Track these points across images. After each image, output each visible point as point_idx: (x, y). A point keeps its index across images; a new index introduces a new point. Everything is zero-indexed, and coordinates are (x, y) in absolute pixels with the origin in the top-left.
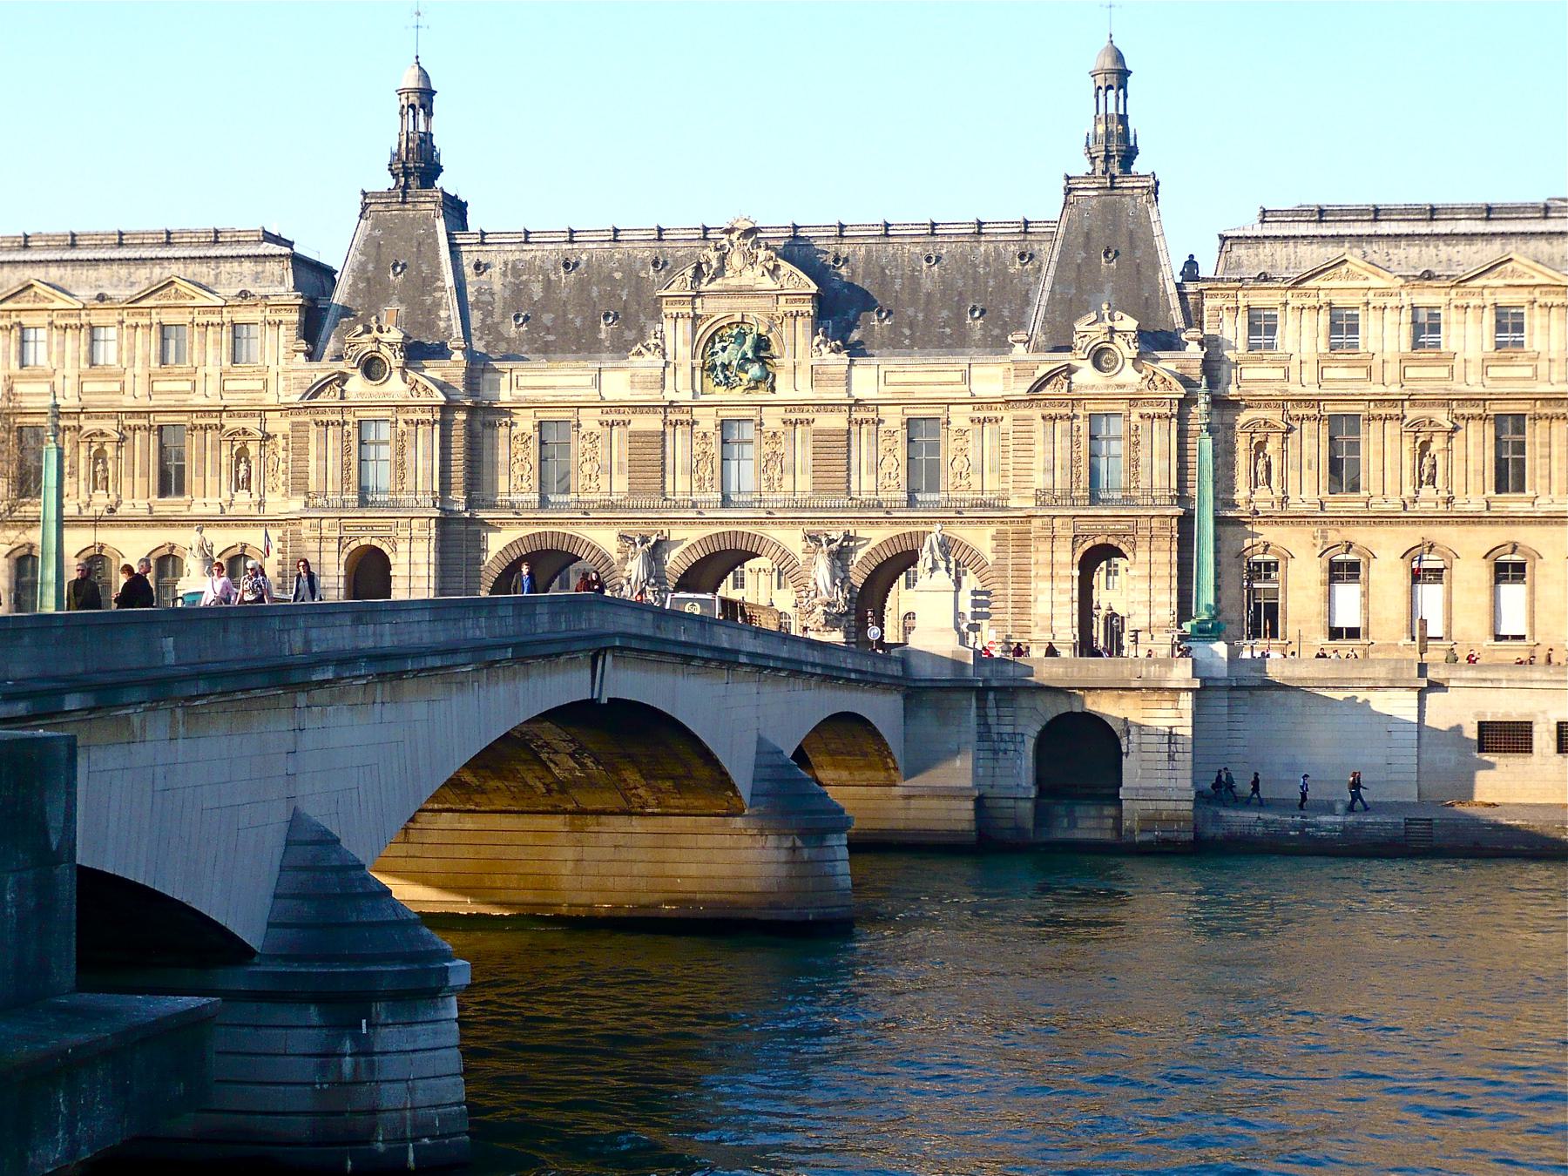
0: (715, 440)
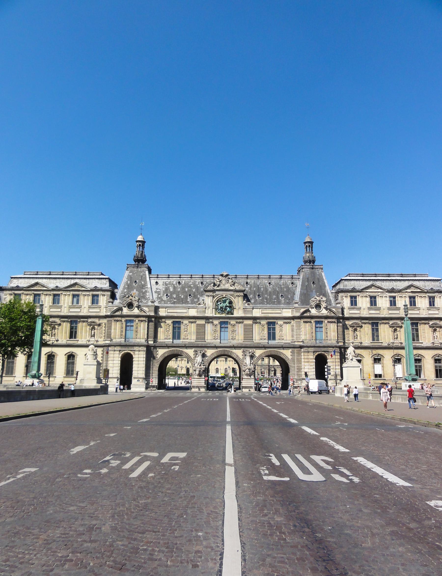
0: (219, 326)
